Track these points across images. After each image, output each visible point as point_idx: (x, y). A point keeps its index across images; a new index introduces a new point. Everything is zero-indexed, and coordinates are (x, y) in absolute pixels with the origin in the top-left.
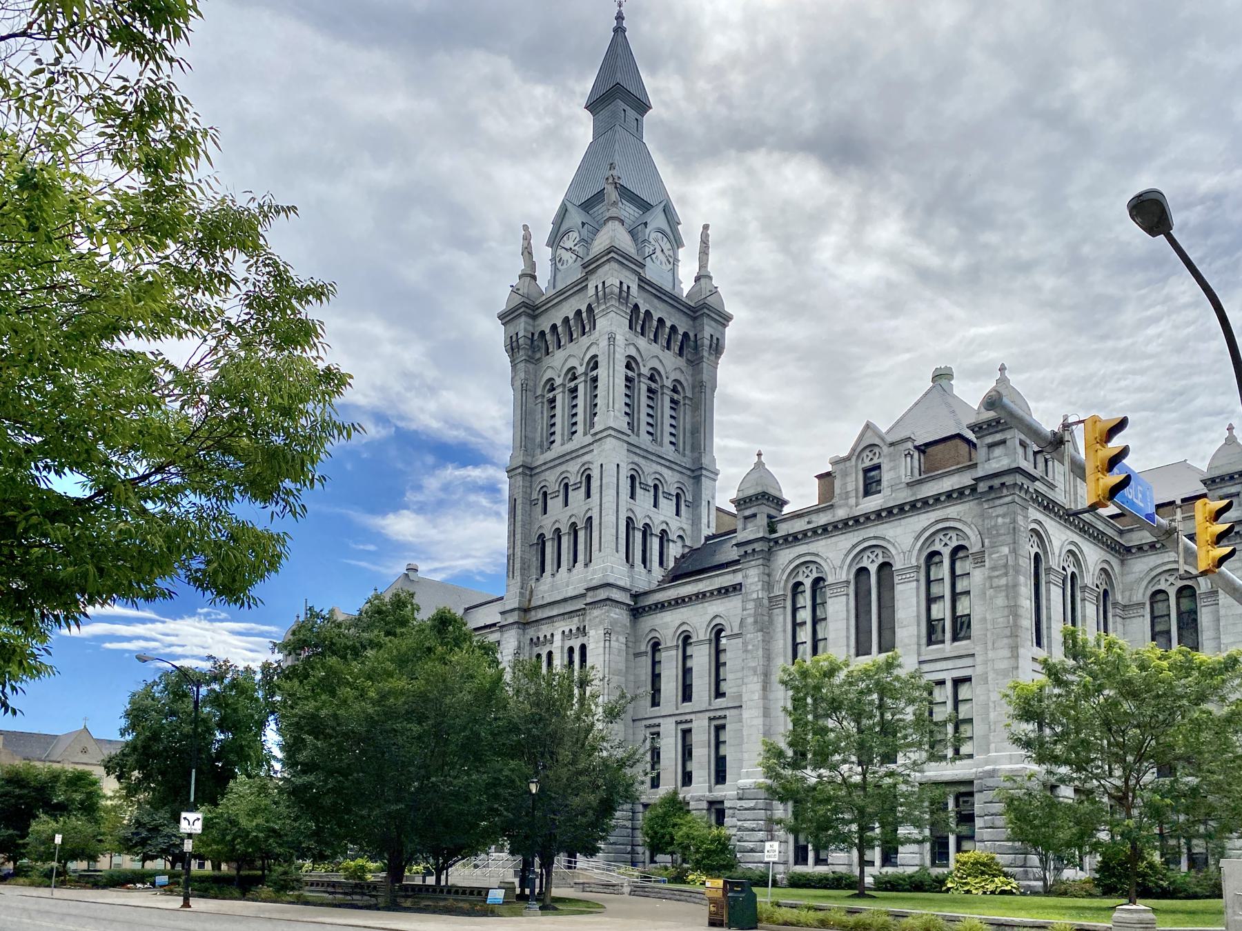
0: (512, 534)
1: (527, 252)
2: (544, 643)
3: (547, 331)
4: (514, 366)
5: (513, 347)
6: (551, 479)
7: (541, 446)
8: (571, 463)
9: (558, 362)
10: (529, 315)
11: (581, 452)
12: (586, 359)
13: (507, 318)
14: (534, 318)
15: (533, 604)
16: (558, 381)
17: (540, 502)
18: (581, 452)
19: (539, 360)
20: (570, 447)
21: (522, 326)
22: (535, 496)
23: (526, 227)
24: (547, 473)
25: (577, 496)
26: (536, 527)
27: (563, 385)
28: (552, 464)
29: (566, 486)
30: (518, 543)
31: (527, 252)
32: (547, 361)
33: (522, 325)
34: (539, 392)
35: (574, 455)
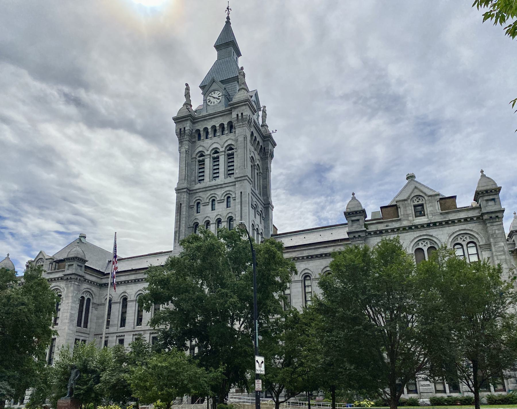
0: (178, 221)
1: (187, 95)
3: (202, 130)
4: (181, 142)
5: (181, 134)
6: (205, 197)
9: (207, 145)
10: (191, 121)
11: (224, 186)
12: (226, 145)
13: (177, 120)
14: (194, 123)
17: (195, 207)
18: (224, 186)
19: (194, 142)
20: (214, 183)
21: (188, 126)
23: (187, 85)
24: (200, 193)
26: (193, 218)
27: (210, 155)
30: (183, 225)
31: (187, 95)
32: (199, 143)
33: (188, 125)
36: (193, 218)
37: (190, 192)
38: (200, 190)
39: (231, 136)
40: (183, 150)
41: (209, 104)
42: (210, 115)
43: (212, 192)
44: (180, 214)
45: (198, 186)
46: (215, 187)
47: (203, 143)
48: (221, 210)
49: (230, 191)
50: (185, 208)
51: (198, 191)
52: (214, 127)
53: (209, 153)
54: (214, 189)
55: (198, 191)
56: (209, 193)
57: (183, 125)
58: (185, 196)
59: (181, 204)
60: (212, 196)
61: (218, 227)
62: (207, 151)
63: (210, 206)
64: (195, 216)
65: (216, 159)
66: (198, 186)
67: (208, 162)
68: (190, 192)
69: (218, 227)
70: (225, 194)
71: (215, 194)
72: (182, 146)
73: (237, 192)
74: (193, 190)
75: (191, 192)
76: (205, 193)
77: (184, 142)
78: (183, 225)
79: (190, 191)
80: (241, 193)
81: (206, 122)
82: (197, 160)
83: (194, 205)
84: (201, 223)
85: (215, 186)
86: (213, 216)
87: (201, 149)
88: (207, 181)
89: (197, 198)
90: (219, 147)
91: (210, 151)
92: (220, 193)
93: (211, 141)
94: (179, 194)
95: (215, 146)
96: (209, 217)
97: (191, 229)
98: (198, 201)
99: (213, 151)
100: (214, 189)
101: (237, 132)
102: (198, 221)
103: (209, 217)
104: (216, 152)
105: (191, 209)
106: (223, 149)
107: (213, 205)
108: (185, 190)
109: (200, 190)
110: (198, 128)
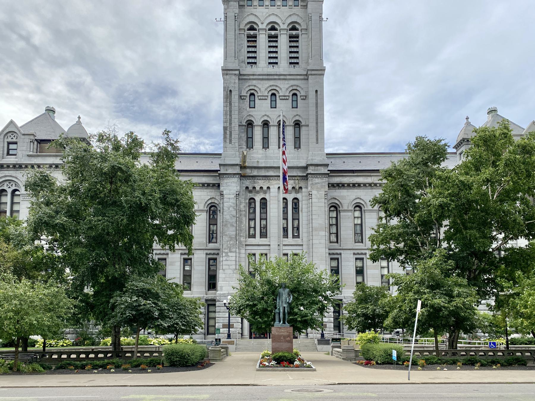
2: (258, 192)
6: (263, 88)
7: (245, 63)
11: (288, 77)
12: (289, 21)
15: (247, 164)
16: (261, 26)
18: (288, 77)
20: (271, 70)
22: (244, 93)
24: (254, 82)
26: (245, 114)
29: (273, 95)
32: (248, 10)
34: (242, 27)
35: (282, 77)
36: (245, 114)
37: (242, 77)
38: (255, 77)
40: (231, 15)
43: (272, 83)
44: (230, 104)
45: (248, 70)
46: (276, 77)
49: (297, 86)
50: (237, 97)
51: (251, 77)
53: (264, 26)
54: (275, 79)
55: (251, 77)
58: (237, 81)
59: (231, 91)
60: (274, 88)
62: (262, 23)
64: (248, 112)
65: (273, 38)
66: (248, 70)
67: (262, 41)
68: (242, 77)
70: (291, 88)
71: (276, 86)
72: (228, 8)
73: (310, 89)
74: (244, 75)
75: (241, 77)
76: (262, 82)
77: (232, 3)
78: (236, 120)
79: (240, 75)
80: (316, 91)
82: (246, 34)
83: (246, 96)
84: (258, 122)
85: (277, 75)
86: (274, 117)
87: (252, 19)
88: (263, 66)
89: (251, 88)
90: (278, 21)
91: (265, 24)
92: (284, 88)
94: (225, 77)
95: (273, 19)
96: (268, 116)
97: (244, 127)
98: (252, 92)
99: (270, 26)
100: (275, 79)
101: (308, 6)
102: (253, 119)
103: (268, 116)
104: (273, 29)
105: (241, 101)
106: (285, 27)
108: (237, 72)
109: (255, 77)
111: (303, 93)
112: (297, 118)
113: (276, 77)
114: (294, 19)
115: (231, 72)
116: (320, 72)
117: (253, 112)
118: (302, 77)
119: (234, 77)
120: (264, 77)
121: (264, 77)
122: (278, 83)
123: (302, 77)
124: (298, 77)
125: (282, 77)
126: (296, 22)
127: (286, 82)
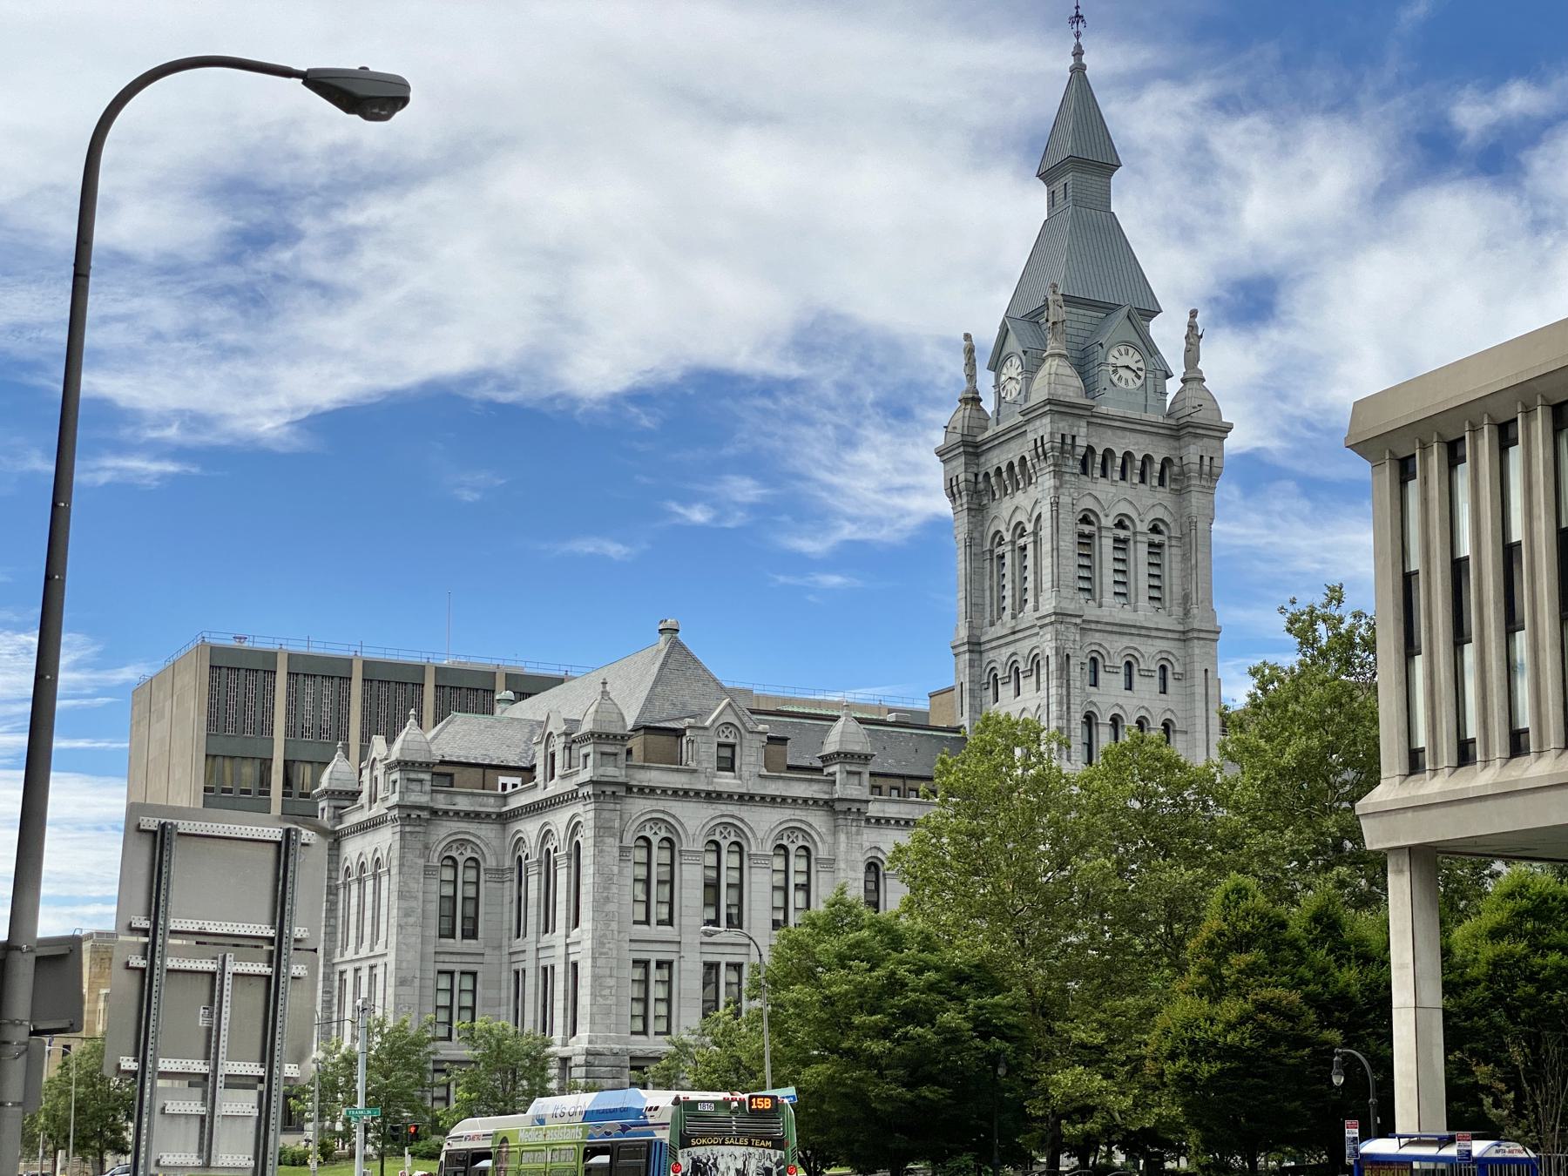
6: (1116, 648)
8: (1116, 637)
25: (1146, 688)
28: (1109, 628)
38: (1099, 627)
39: (1163, 495)
41: (1115, 379)
42: (1125, 420)
46: (1133, 631)
47: (1090, 485)
48: (1145, 699)
51: (1093, 626)
52: (1128, 456)
55: (1093, 626)
56: (1126, 641)
57: (1071, 427)
61: (1116, 739)
63: (1122, 677)
69: (1116, 739)
81: (1110, 432)
87: (1088, 503)
93: (1113, 489)
107: (1129, 676)
109: (1099, 627)
110: (1094, 442)
111: (1178, 669)
112: (1168, 715)
113: (1133, 631)
114: (1159, 513)
115: (1068, 619)
116: (1212, 636)
117: (1096, 695)
118: (1176, 636)
119: (1073, 629)
120: (1115, 629)
121: (1115, 629)
122: (1136, 642)
123: (1176, 636)
124: (1170, 635)
125: (1143, 632)
126: (1161, 520)
127: (1150, 641)
